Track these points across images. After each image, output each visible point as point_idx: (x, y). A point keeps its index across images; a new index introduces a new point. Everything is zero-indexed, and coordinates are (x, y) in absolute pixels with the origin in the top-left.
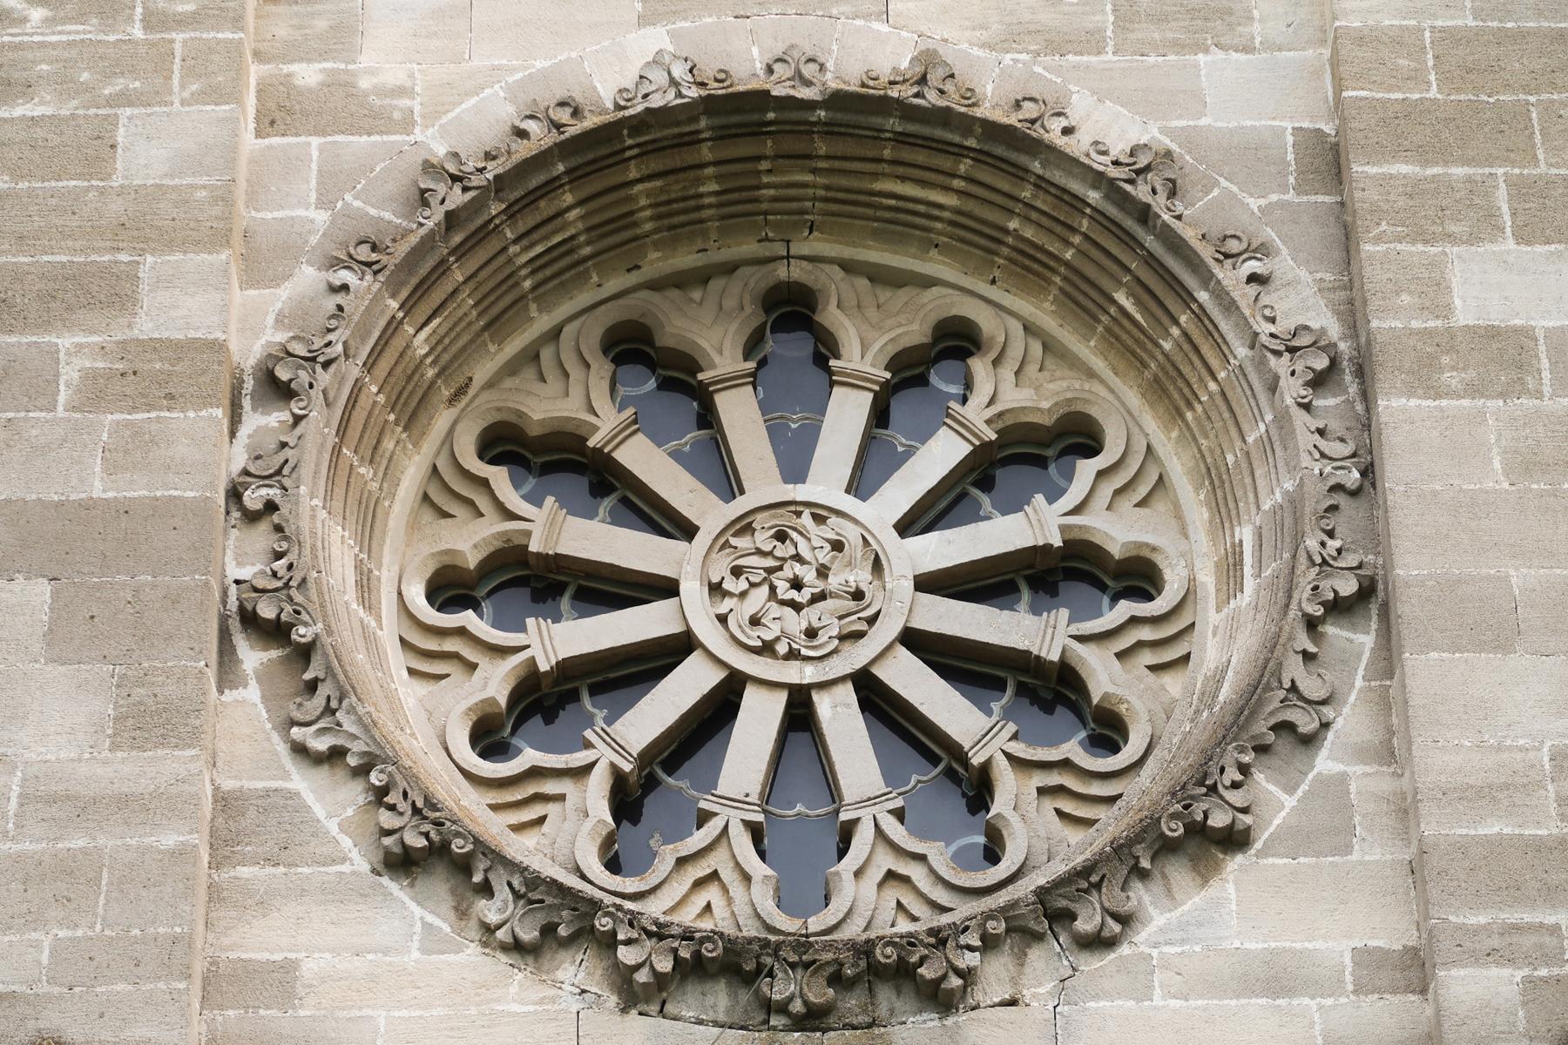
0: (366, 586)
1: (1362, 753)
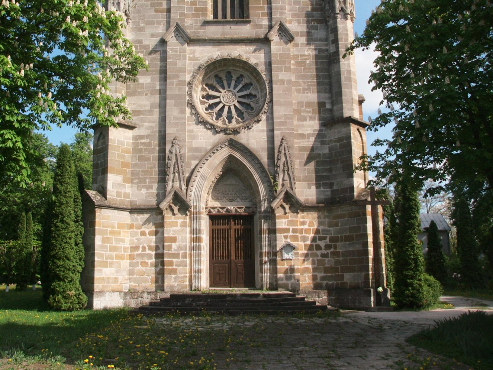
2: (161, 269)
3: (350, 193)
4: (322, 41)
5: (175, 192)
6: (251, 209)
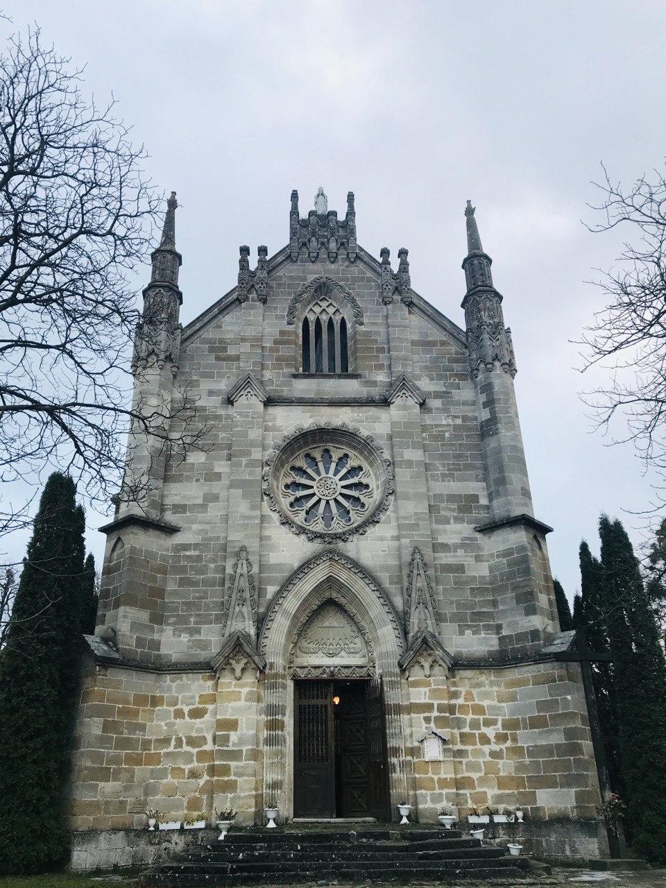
0: (278, 488)
6: (365, 669)
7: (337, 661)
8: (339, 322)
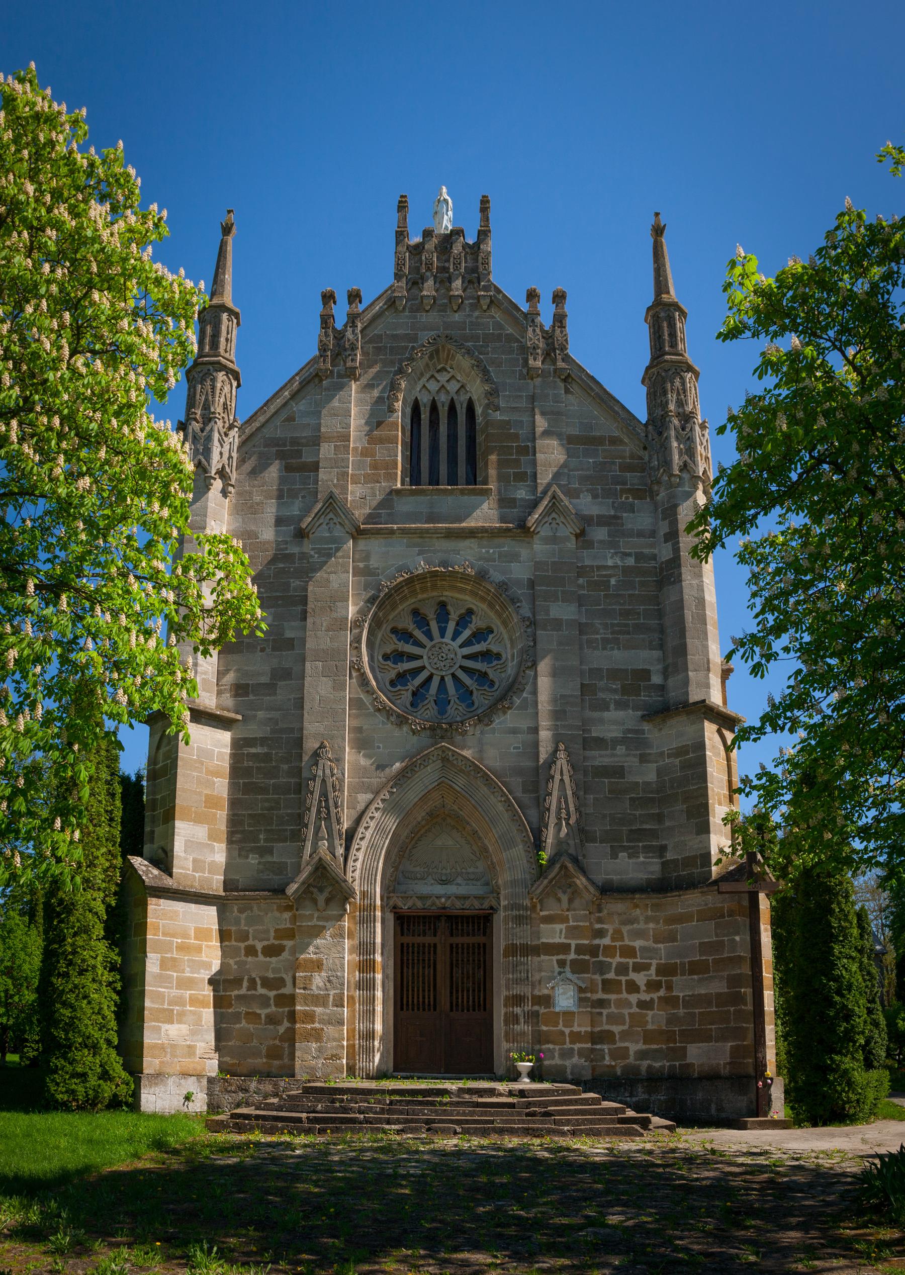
1: (531, 693)
2: (288, 1029)
3: (702, 867)
4: (644, 536)
5: (320, 859)
7: (452, 889)
8: (465, 405)
